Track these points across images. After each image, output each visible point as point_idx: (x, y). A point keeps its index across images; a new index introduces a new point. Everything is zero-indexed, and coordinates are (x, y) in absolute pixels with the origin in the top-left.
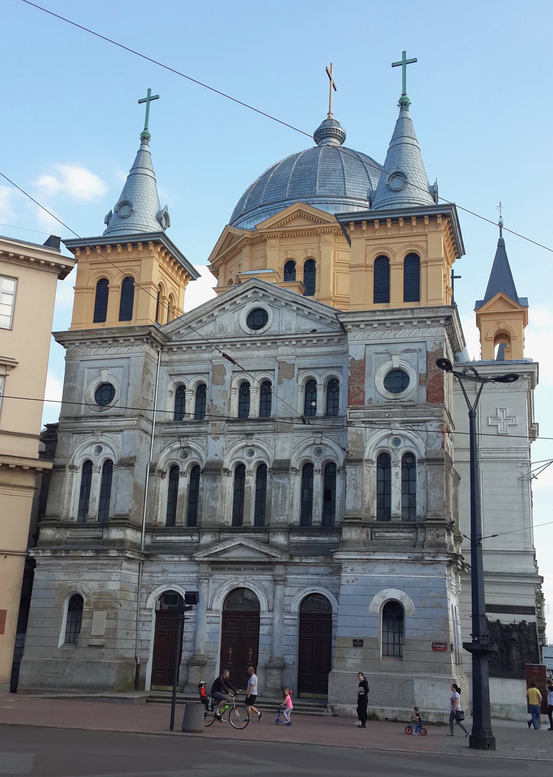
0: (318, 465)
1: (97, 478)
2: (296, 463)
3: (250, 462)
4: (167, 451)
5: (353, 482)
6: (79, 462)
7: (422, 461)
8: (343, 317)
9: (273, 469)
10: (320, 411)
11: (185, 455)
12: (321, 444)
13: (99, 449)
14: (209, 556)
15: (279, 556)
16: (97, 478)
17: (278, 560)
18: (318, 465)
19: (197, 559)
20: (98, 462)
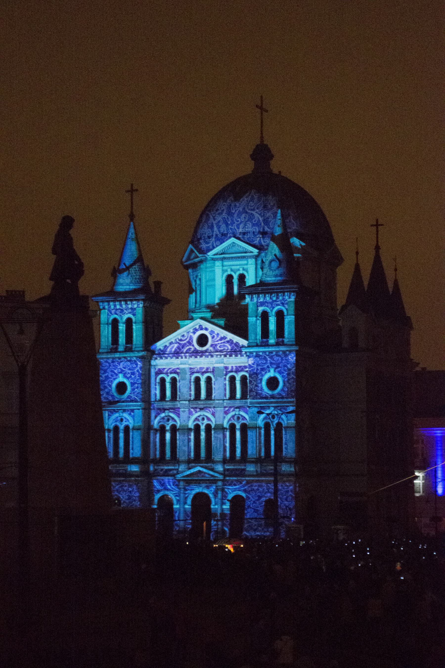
0: (238, 426)
1: (121, 435)
2: (226, 425)
3: (203, 424)
4: (158, 418)
5: (252, 439)
6: (111, 427)
7: (285, 427)
8: (244, 349)
9: (214, 428)
10: (238, 395)
11: (168, 420)
12: (239, 414)
13: (122, 420)
14: (184, 477)
15: (218, 476)
16: (121, 435)
17: (219, 478)
18: (238, 426)
19: (177, 478)
20: (122, 427)
